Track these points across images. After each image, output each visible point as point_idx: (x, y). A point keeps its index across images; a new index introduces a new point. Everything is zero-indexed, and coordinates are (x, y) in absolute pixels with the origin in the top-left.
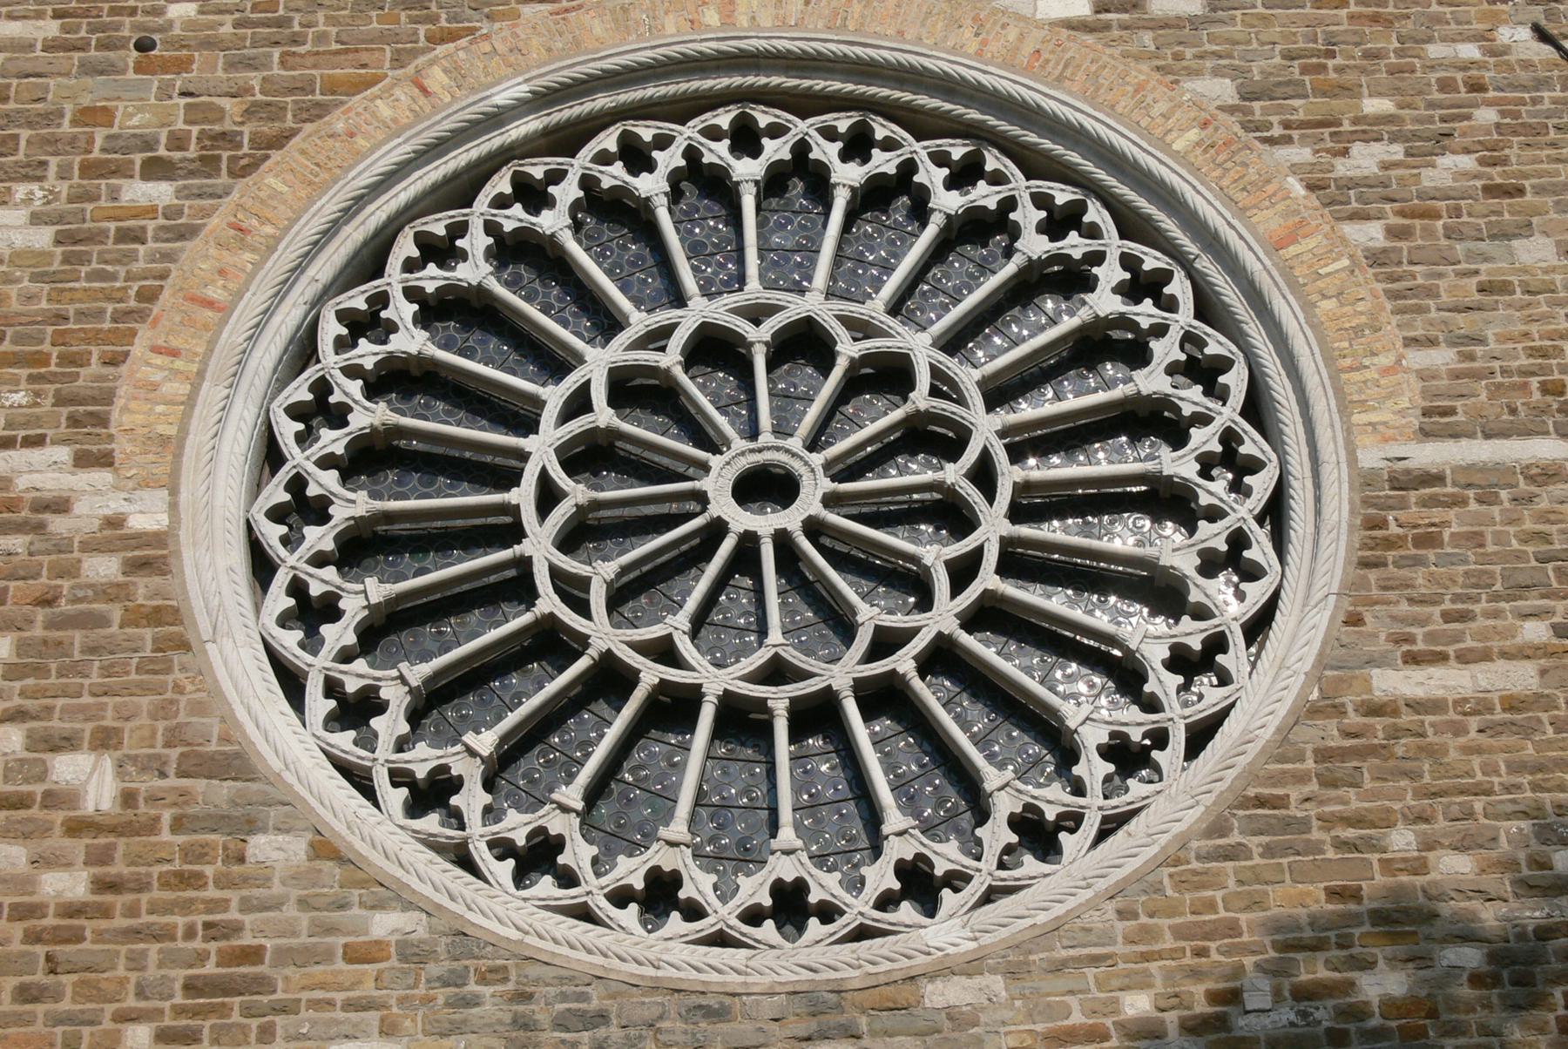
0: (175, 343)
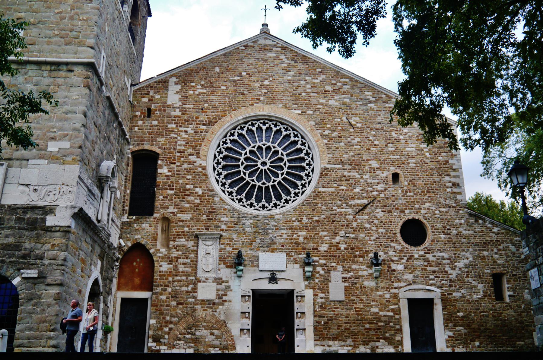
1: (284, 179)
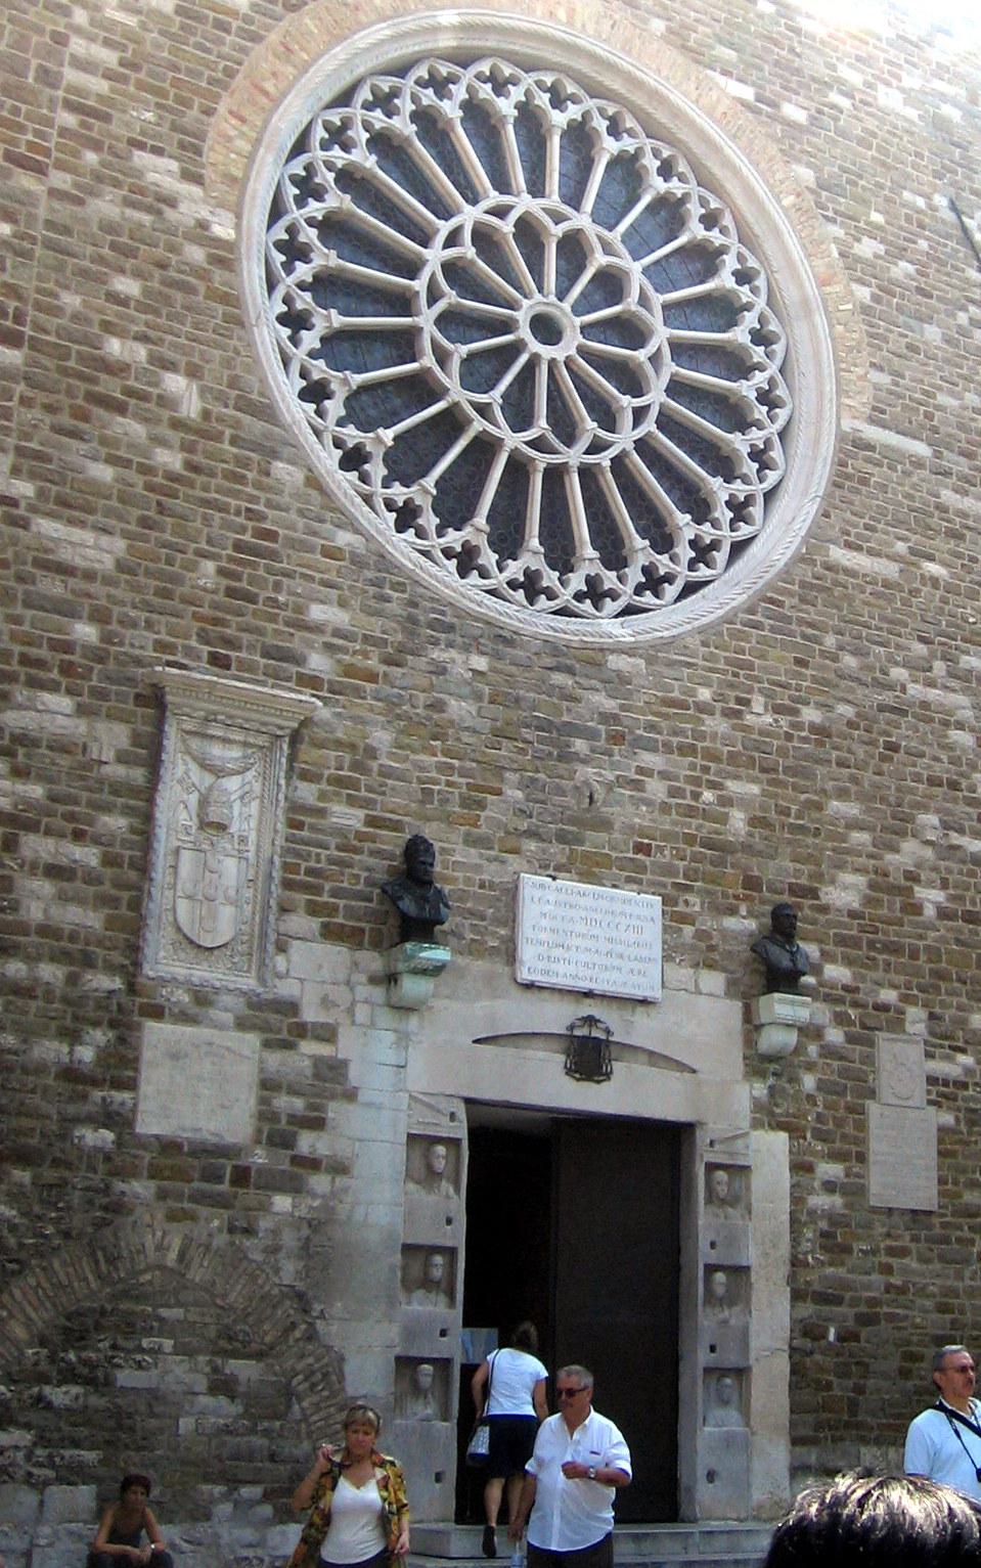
0: (246, 112)
1: (642, 445)
